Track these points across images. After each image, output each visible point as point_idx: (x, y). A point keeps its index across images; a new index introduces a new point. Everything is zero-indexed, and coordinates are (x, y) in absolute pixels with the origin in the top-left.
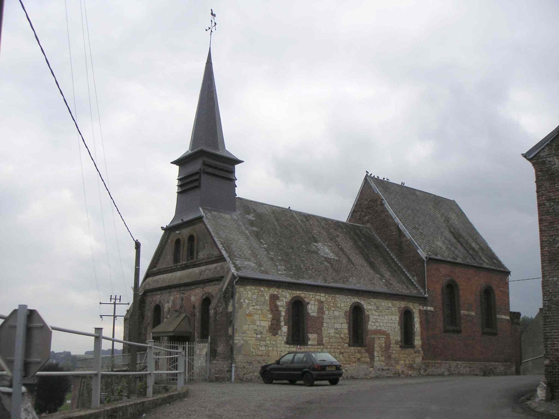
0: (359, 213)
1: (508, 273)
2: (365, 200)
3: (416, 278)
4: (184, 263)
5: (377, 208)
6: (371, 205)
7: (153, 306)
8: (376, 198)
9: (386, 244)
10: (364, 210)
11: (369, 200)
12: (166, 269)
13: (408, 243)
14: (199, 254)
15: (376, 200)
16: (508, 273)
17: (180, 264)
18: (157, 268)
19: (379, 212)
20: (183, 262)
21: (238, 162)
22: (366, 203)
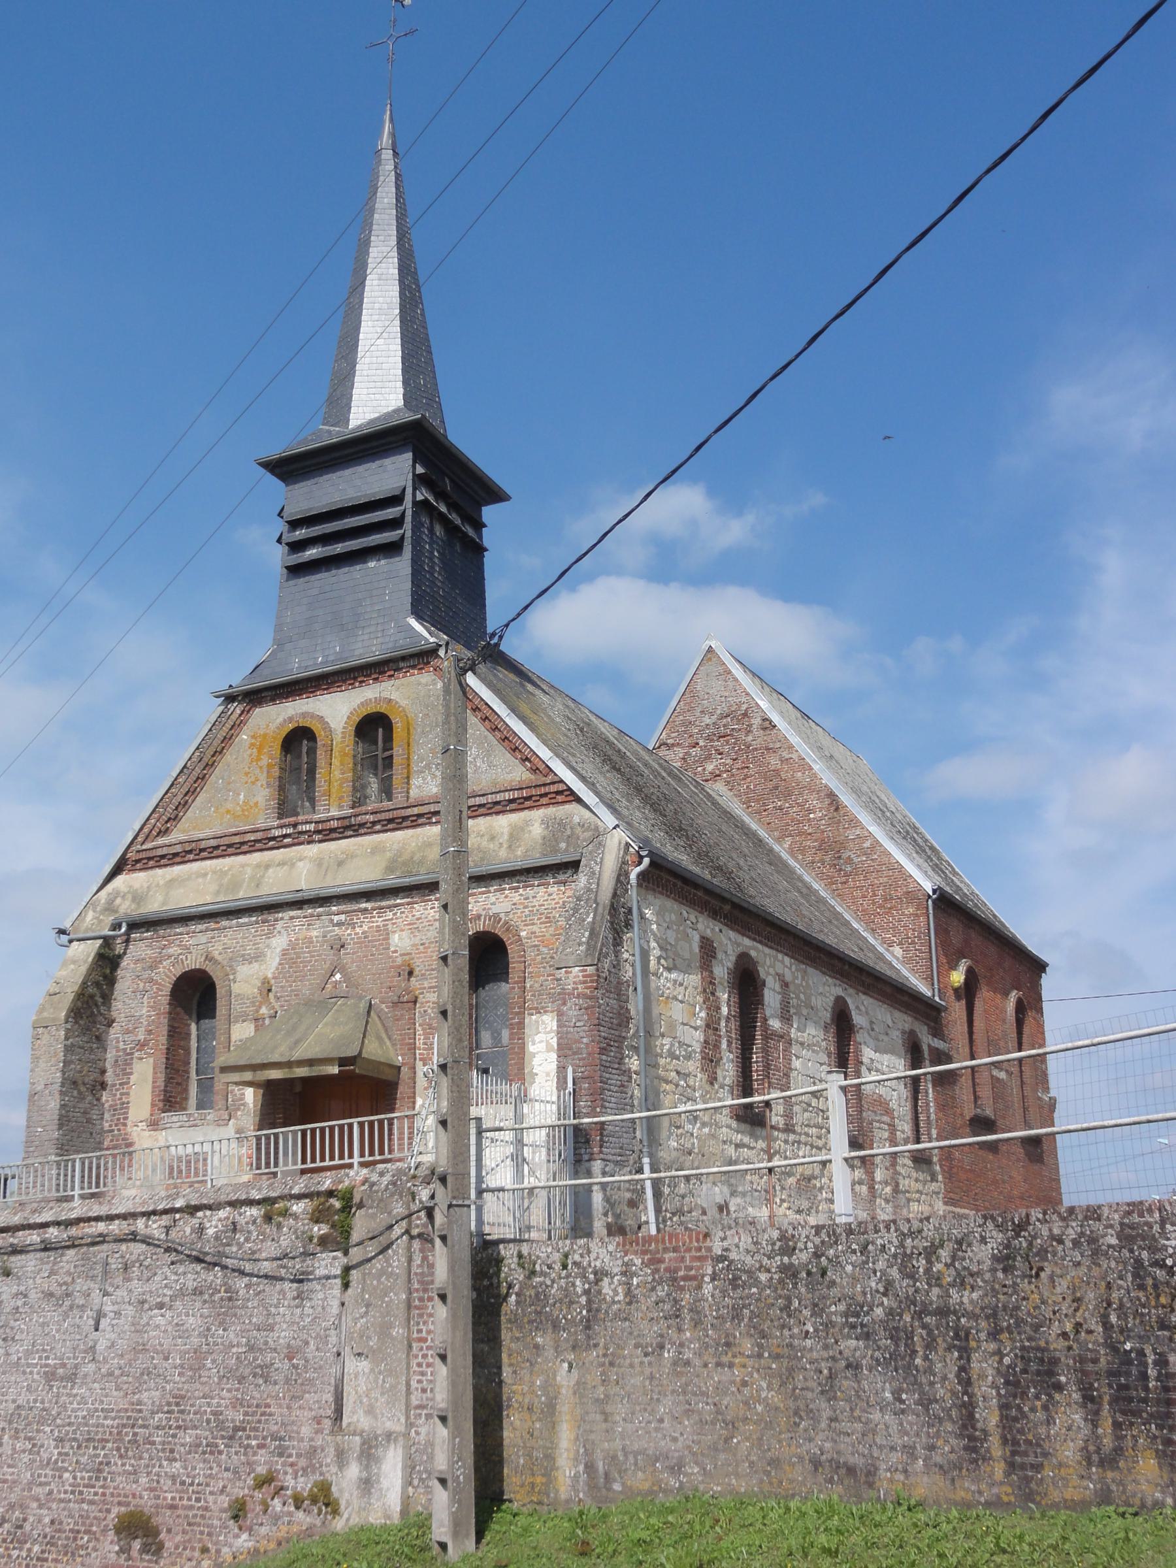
0: (680, 752)
1: (1039, 967)
2: (702, 712)
3: (898, 951)
4: (334, 813)
5: (750, 738)
6: (724, 726)
7: (167, 974)
8: (744, 707)
9: (786, 846)
10: (702, 743)
11: (719, 712)
12: (237, 839)
13: (867, 844)
14: (416, 782)
15: (745, 715)
16: (1039, 967)
17: (316, 817)
18: (176, 835)
19: (756, 749)
20: (333, 809)
21: (496, 495)
22: (707, 720)
